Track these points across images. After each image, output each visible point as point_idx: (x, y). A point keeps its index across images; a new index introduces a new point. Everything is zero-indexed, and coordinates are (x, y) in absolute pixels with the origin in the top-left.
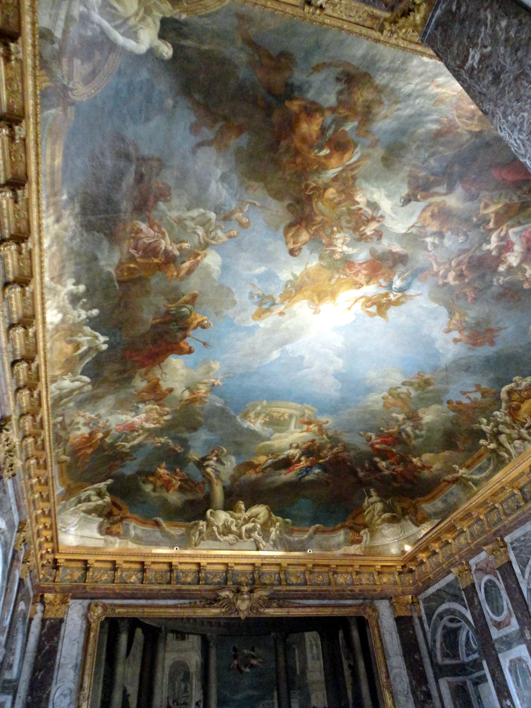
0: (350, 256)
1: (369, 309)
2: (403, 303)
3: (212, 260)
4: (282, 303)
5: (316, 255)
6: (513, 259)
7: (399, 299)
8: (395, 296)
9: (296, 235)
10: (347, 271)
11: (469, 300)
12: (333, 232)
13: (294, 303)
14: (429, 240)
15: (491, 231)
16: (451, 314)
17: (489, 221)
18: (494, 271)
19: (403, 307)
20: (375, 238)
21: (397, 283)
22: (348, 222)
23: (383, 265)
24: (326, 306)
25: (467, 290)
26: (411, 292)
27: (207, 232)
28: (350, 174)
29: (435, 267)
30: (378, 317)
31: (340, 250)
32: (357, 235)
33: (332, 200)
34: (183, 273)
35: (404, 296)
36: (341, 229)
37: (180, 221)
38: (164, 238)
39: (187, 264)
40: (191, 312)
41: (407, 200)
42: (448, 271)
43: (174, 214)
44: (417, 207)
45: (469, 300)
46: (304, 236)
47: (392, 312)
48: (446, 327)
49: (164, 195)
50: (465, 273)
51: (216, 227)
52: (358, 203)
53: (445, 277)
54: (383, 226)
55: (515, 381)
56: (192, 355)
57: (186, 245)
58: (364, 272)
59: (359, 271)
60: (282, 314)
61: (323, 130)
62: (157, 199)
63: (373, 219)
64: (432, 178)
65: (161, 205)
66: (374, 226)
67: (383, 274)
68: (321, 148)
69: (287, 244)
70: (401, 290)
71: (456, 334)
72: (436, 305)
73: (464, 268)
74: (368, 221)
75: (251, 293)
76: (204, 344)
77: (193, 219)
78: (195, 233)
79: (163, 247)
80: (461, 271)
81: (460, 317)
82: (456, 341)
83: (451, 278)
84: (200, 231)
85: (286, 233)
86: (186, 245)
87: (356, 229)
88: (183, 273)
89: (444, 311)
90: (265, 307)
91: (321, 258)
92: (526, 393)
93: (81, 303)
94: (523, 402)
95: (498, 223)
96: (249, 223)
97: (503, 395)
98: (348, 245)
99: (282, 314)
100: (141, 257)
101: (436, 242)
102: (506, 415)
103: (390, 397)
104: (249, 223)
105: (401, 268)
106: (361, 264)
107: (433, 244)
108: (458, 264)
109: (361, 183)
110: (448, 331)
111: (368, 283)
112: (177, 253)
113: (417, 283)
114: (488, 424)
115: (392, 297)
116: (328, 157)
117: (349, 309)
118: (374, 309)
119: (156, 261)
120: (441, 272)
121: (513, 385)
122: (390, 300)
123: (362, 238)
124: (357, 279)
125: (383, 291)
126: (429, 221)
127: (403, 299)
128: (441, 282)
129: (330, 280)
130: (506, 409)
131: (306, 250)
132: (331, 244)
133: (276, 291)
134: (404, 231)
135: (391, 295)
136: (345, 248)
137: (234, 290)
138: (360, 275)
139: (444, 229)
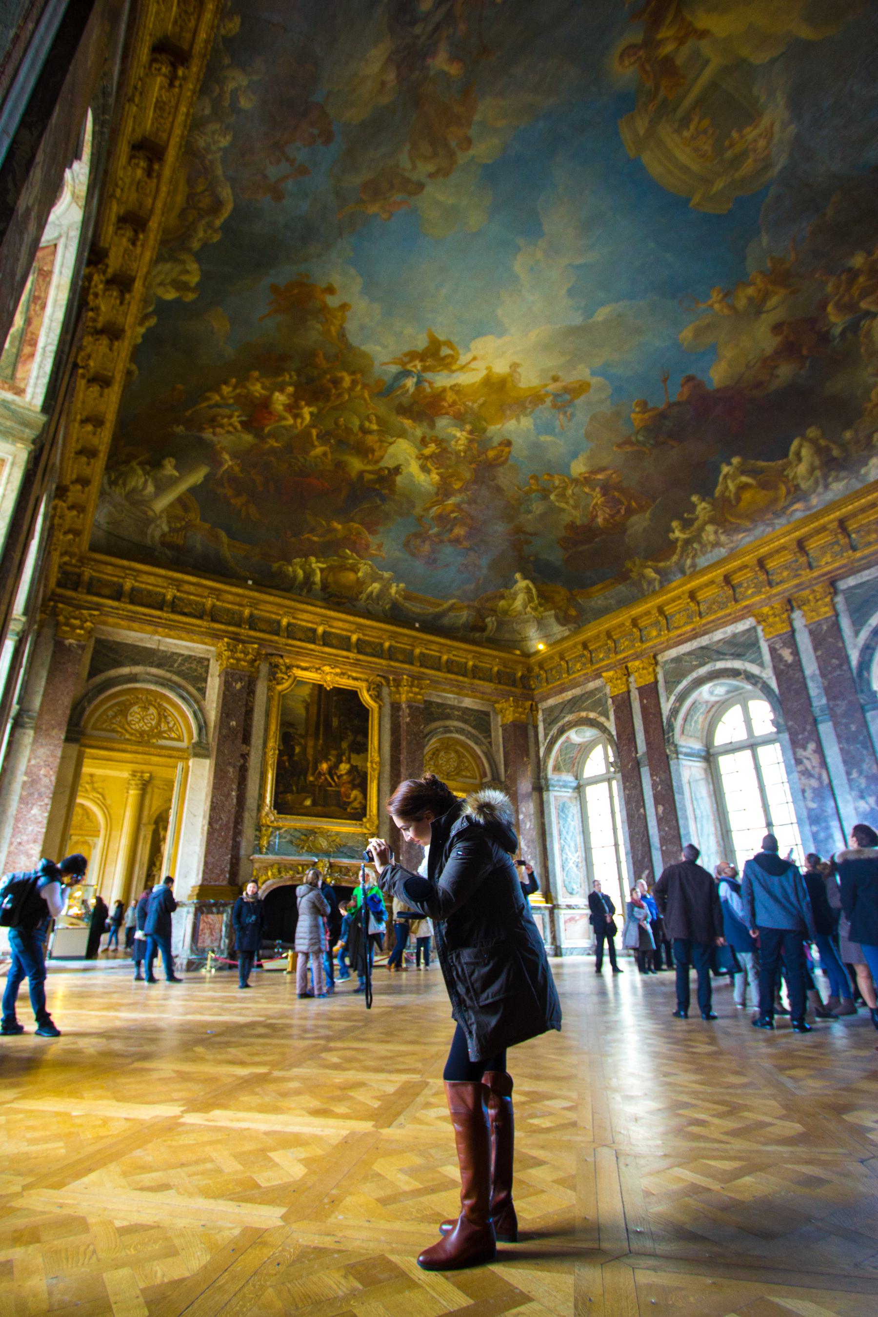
0: (456, 426)
1: (449, 352)
2: (406, 355)
3: (578, 468)
4: (547, 394)
5: (488, 434)
6: (280, 399)
7: (411, 361)
8: (415, 366)
9: (497, 457)
10: (462, 409)
11: (321, 355)
12: (465, 452)
13: (535, 388)
14: (375, 427)
15: (312, 425)
16: (342, 335)
17: (317, 436)
18: (297, 386)
19: (406, 348)
20: (428, 439)
21: (410, 383)
22: (449, 459)
23: (426, 408)
24: (501, 368)
25: (324, 364)
26: (394, 369)
27: (565, 489)
28: (440, 498)
29: (366, 395)
30: (442, 338)
31: (464, 433)
32: (444, 445)
33: (458, 479)
34: (609, 472)
35: (404, 364)
36: (457, 454)
37: (575, 507)
38: (596, 504)
39: (600, 477)
40: (638, 432)
41: (397, 470)
42: (352, 389)
43: (576, 513)
44: (388, 463)
45: (321, 355)
46: (491, 454)
47: (421, 343)
48: (348, 314)
49: (572, 526)
50: (331, 386)
51: (557, 488)
52: (438, 474)
53: (354, 383)
54: (419, 450)
55: (216, 231)
56: (691, 372)
57: (587, 490)
58: (445, 404)
59: (450, 406)
60: (555, 379)
61: (451, 530)
62: (577, 527)
63: (427, 458)
64: (377, 486)
65: (578, 523)
66: (427, 452)
67: (425, 397)
68: (455, 518)
69: (510, 452)
70: (407, 373)
71: (333, 302)
72: (363, 348)
73: (334, 391)
74: (431, 457)
75: (570, 420)
76: (665, 381)
77: (567, 503)
78: (573, 494)
79: (602, 499)
80: (336, 388)
81: (329, 331)
82: (330, 290)
83: (347, 380)
84: (570, 492)
85: (507, 459)
86: (587, 490)
87: (444, 450)
88: (609, 472)
89: (354, 339)
90: (568, 397)
91: (484, 430)
92: (191, 218)
93: (690, 516)
94: (190, 197)
95: (306, 433)
96: (532, 478)
97: (226, 193)
98: (455, 437)
99: (555, 379)
100: (622, 503)
101: (367, 424)
102: (208, 149)
103: (453, 144)
104: (532, 478)
105: (405, 401)
106: (447, 414)
107: (370, 422)
108: (340, 395)
109: (432, 489)
110: (344, 307)
111: (444, 390)
112: (598, 489)
113: (388, 379)
114: (234, 92)
115: (419, 365)
116: (453, 512)
117: (474, 359)
118: (445, 351)
119: (616, 494)
120: (359, 388)
121: (218, 223)
122: (422, 360)
123: (439, 442)
124: (455, 397)
125: (428, 376)
126: (376, 446)
127: (406, 359)
128: (359, 376)
129: (483, 405)
130: (212, 162)
131: (496, 442)
132: (471, 441)
133: (545, 410)
134: (400, 440)
135: (419, 367)
136: (458, 434)
137: (583, 431)
138: (450, 400)
139: (360, 435)
